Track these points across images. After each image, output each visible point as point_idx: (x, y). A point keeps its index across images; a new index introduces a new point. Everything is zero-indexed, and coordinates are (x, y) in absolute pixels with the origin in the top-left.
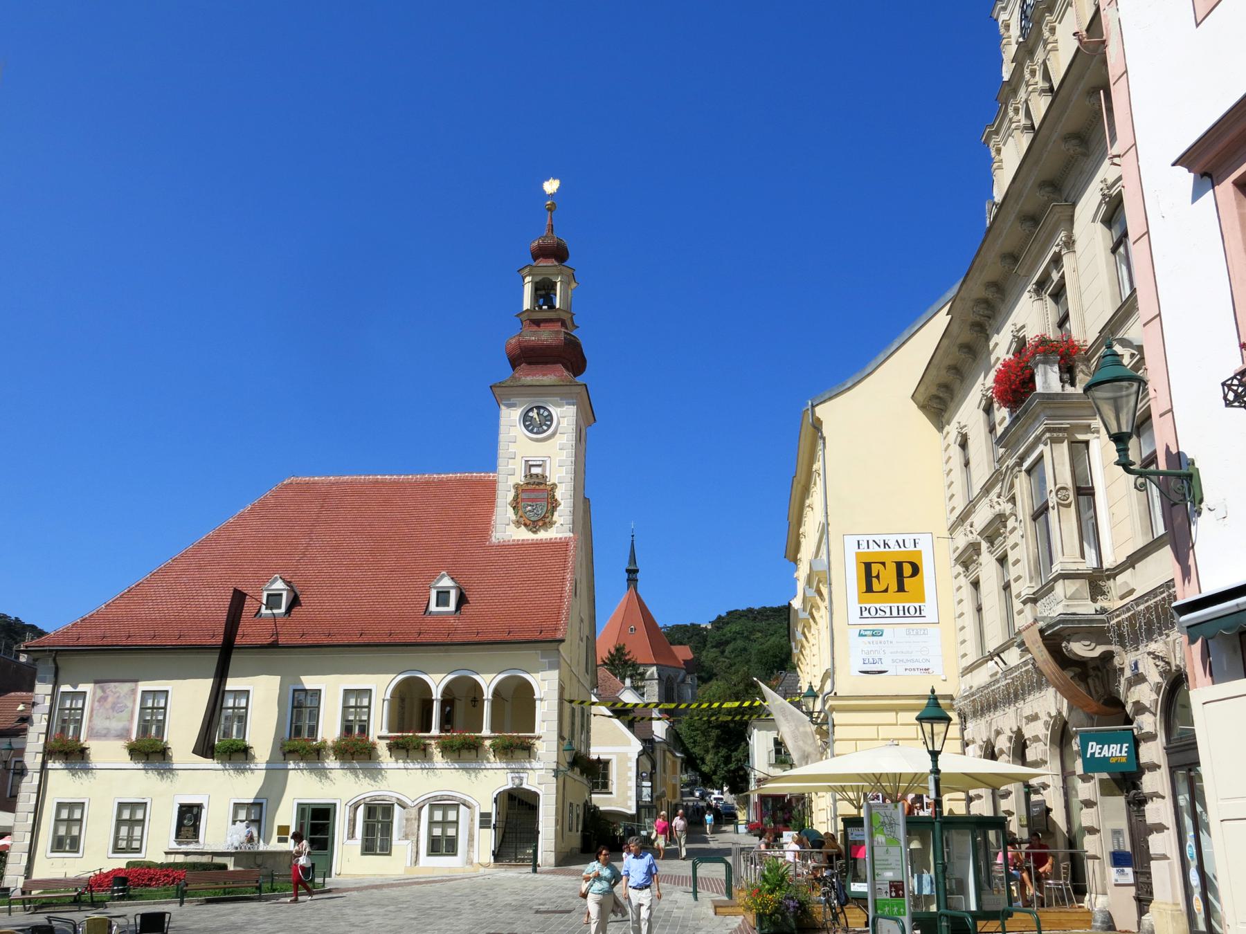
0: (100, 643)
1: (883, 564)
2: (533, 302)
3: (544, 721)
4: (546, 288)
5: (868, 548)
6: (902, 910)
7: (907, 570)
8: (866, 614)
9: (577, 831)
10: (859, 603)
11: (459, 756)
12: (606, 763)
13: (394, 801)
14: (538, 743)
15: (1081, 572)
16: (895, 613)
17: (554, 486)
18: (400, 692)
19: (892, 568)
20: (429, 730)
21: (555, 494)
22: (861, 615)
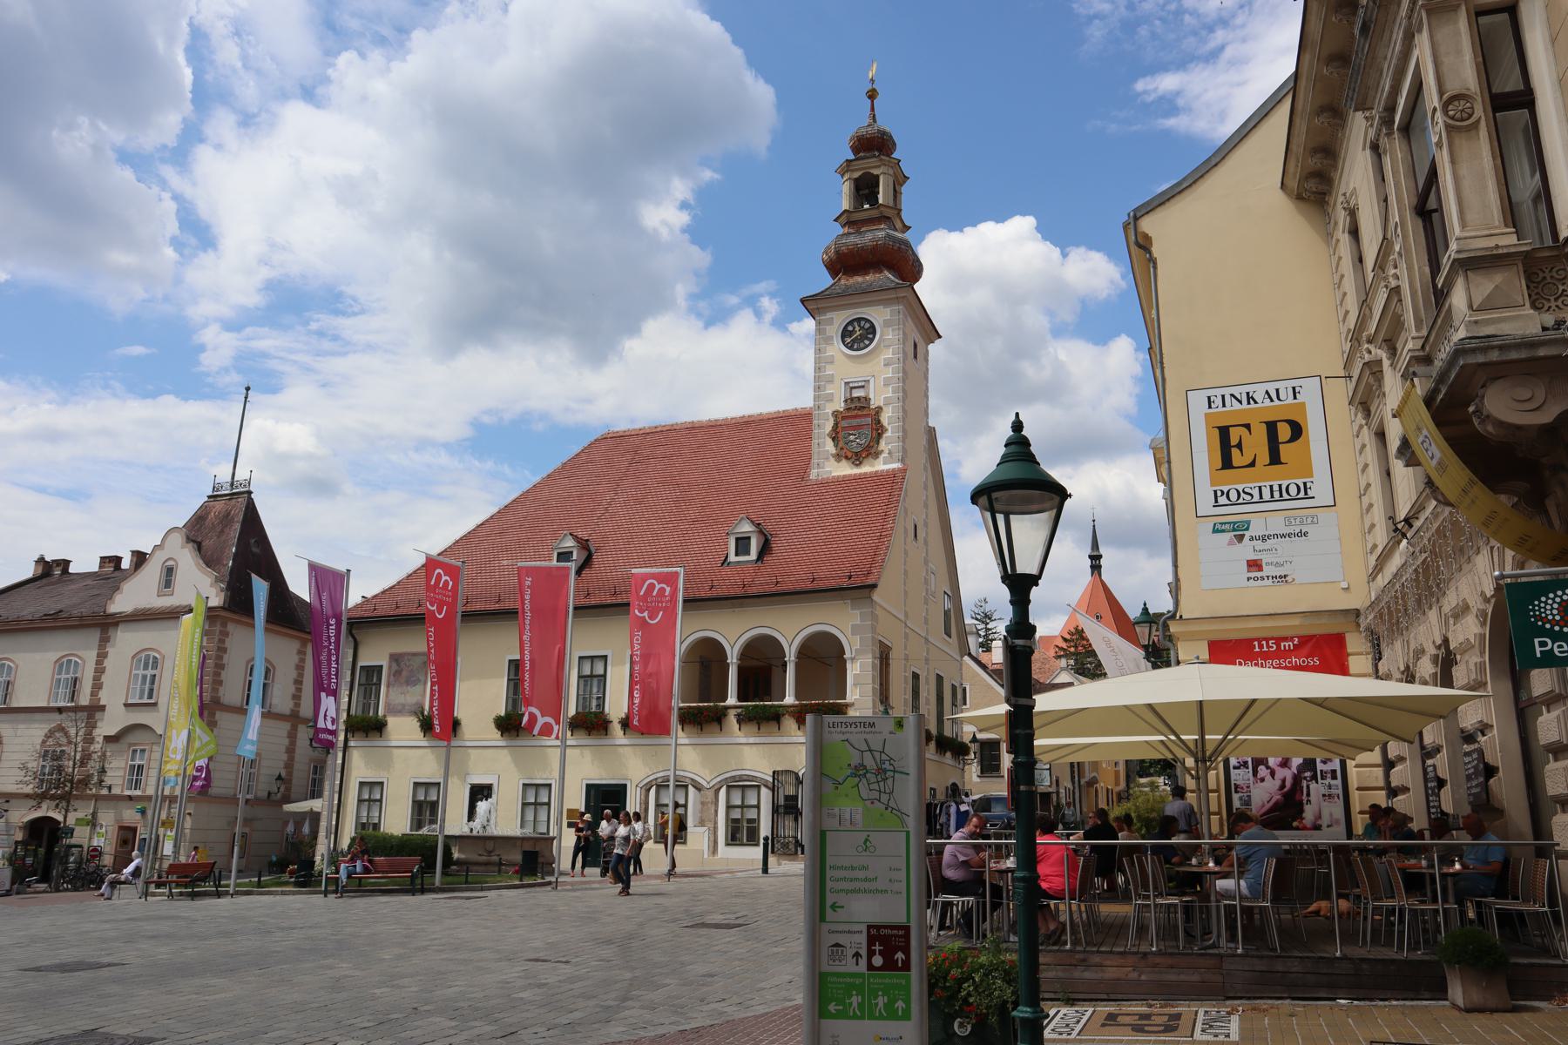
0: (391, 613)
1: (1248, 426)
5: (1224, 405)
7: (1284, 432)
8: (1223, 500)
10: (1212, 485)
11: (759, 729)
13: (688, 781)
15: (1505, 251)
16: (1266, 495)
19: (1261, 433)
21: (882, 419)
22: (1216, 501)
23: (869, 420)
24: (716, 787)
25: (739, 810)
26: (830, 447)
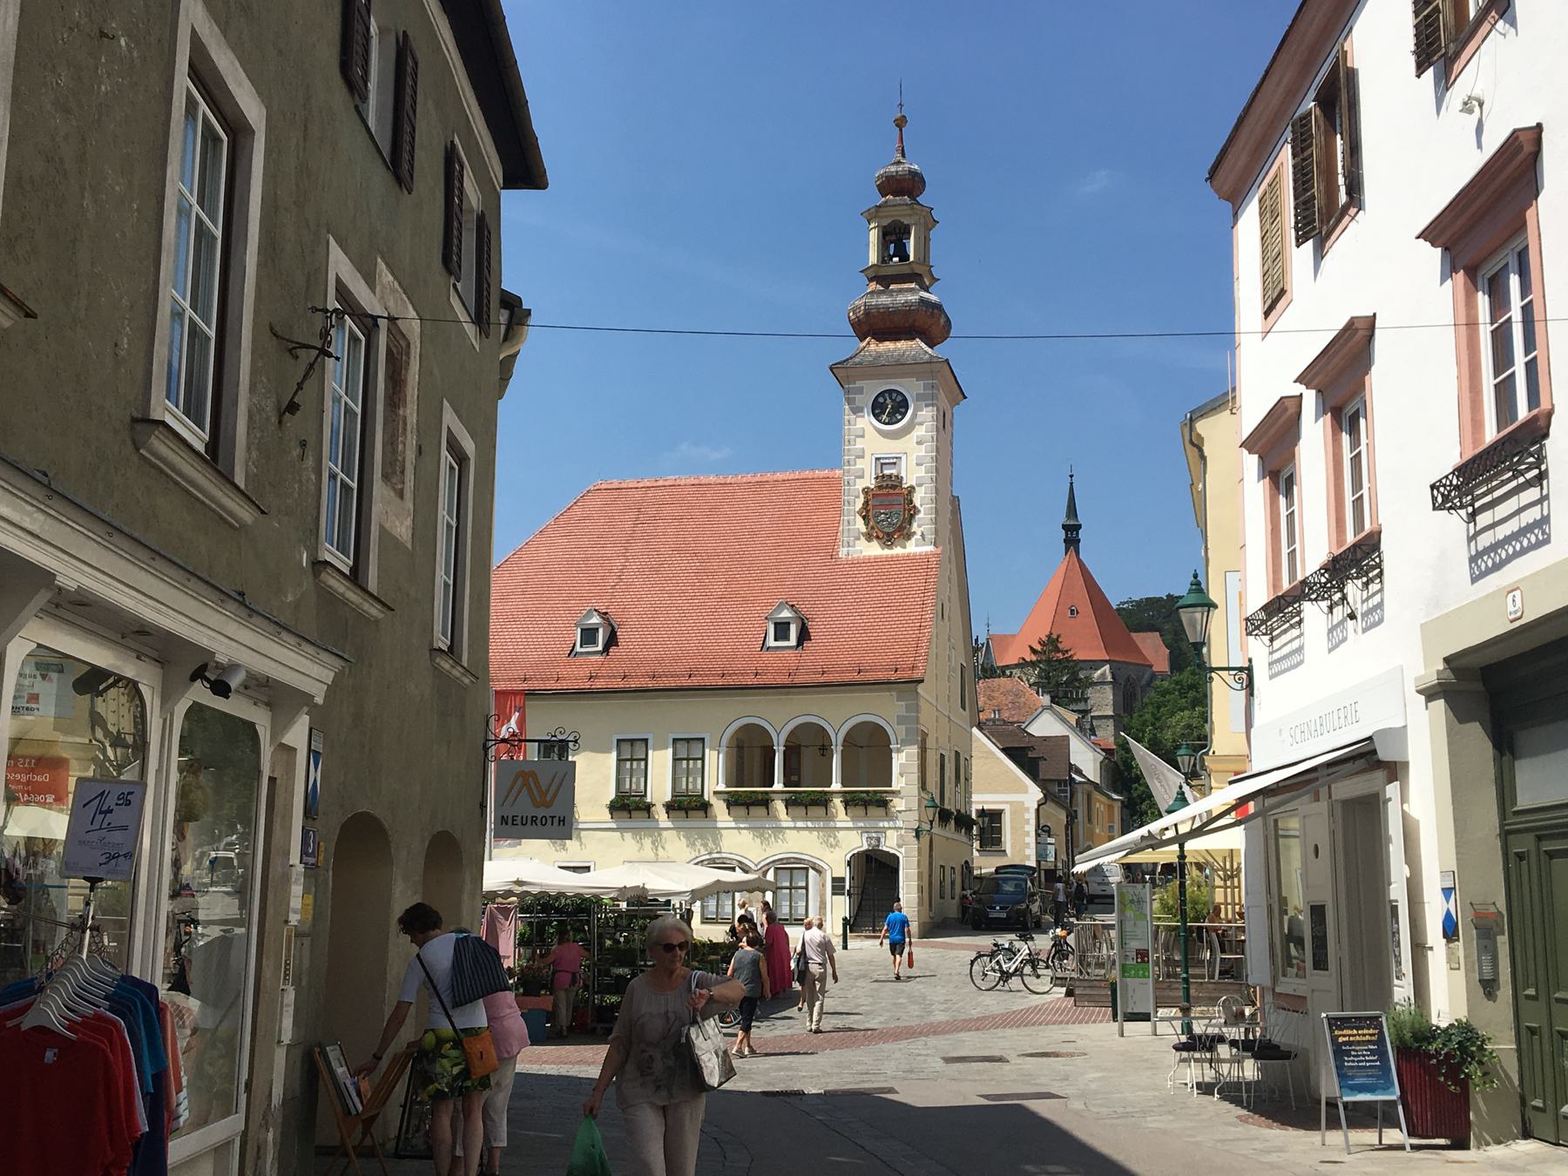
9: (953, 898)
12: (994, 816)
13: (735, 864)
14: (896, 801)
17: (912, 489)
24: (764, 869)
25: (788, 891)
26: (860, 525)
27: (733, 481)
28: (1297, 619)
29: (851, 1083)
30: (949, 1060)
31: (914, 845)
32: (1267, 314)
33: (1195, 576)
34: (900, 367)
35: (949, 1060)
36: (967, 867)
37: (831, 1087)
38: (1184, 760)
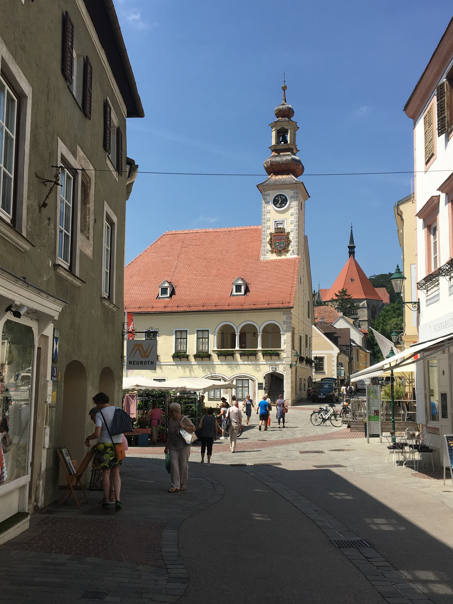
2: (276, 140)
3: (285, 344)
4: (283, 132)
6: (378, 419)
13: (221, 377)
14: (283, 354)
17: (289, 233)
18: (221, 330)
20: (235, 348)
21: (289, 237)
23: (284, 237)
24: (232, 380)
25: (241, 388)
27: (219, 231)
28: (437, 283)
29: (264, 461)
30: (301, 452)
31: (289, 370)
32: (427, 163)
33: (398, 267)
34: (284, 185)
35: (301, 452)
36: (310, 379)
37: (256, 463)
38: (394, 338)
